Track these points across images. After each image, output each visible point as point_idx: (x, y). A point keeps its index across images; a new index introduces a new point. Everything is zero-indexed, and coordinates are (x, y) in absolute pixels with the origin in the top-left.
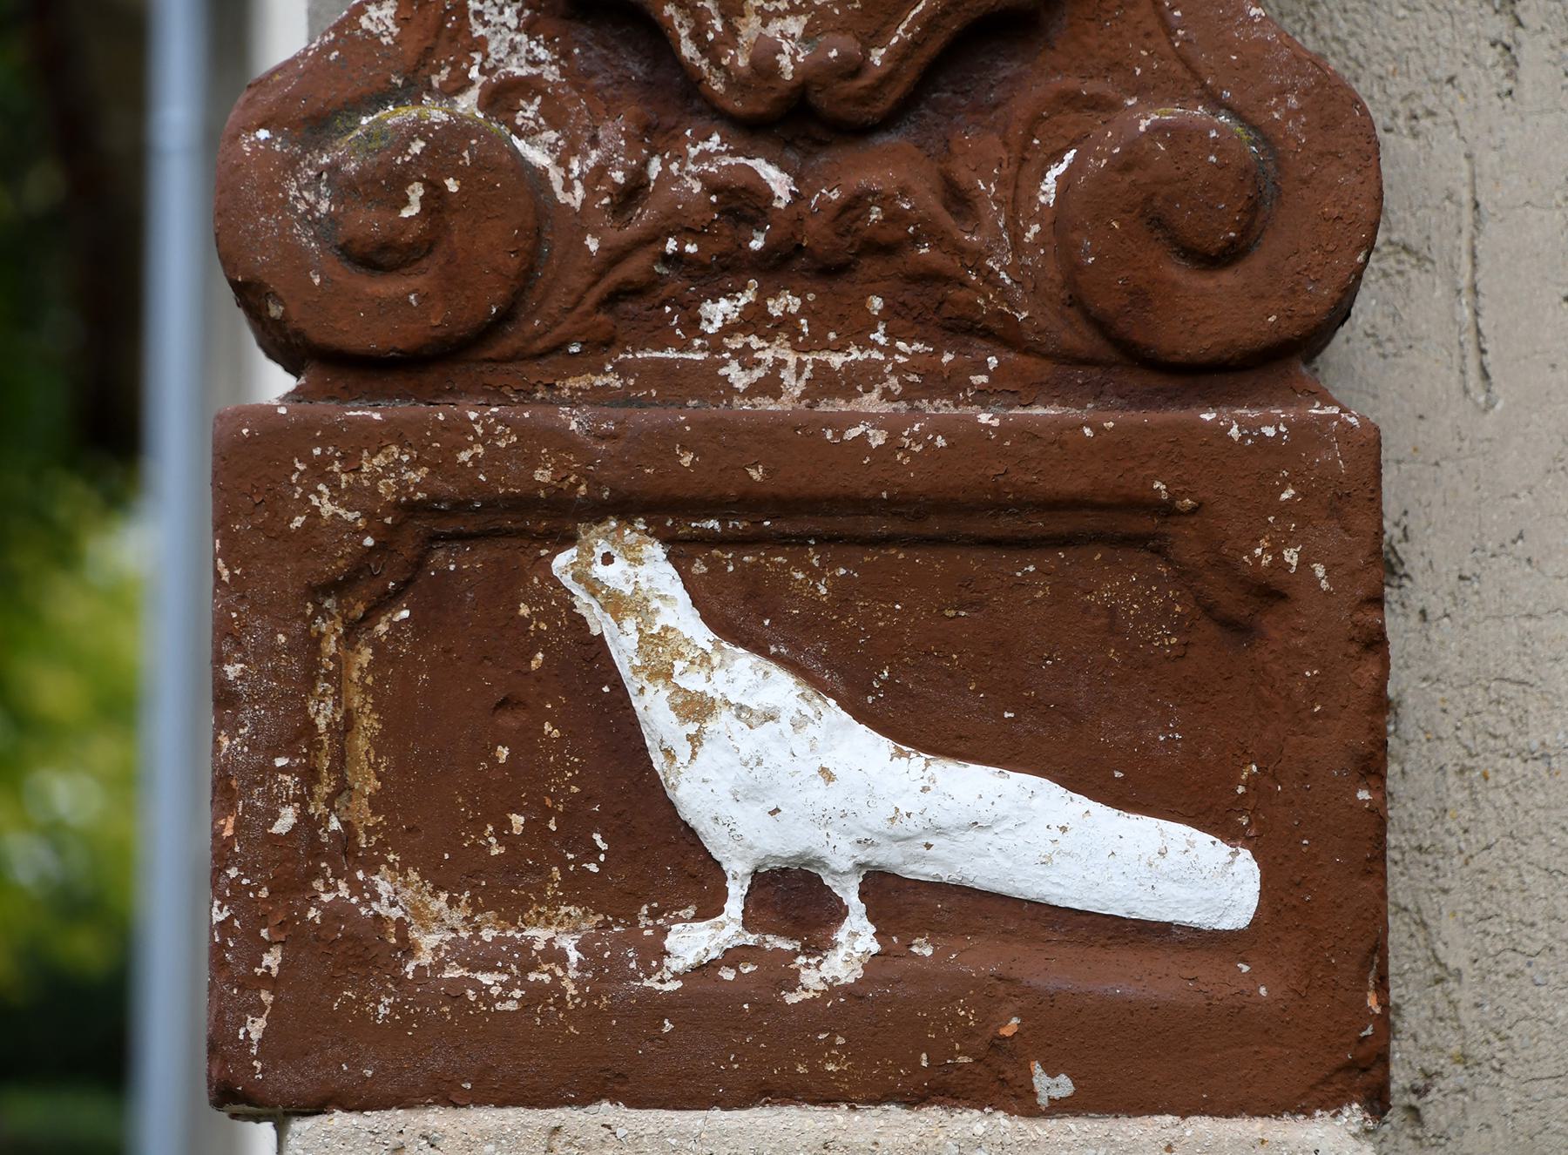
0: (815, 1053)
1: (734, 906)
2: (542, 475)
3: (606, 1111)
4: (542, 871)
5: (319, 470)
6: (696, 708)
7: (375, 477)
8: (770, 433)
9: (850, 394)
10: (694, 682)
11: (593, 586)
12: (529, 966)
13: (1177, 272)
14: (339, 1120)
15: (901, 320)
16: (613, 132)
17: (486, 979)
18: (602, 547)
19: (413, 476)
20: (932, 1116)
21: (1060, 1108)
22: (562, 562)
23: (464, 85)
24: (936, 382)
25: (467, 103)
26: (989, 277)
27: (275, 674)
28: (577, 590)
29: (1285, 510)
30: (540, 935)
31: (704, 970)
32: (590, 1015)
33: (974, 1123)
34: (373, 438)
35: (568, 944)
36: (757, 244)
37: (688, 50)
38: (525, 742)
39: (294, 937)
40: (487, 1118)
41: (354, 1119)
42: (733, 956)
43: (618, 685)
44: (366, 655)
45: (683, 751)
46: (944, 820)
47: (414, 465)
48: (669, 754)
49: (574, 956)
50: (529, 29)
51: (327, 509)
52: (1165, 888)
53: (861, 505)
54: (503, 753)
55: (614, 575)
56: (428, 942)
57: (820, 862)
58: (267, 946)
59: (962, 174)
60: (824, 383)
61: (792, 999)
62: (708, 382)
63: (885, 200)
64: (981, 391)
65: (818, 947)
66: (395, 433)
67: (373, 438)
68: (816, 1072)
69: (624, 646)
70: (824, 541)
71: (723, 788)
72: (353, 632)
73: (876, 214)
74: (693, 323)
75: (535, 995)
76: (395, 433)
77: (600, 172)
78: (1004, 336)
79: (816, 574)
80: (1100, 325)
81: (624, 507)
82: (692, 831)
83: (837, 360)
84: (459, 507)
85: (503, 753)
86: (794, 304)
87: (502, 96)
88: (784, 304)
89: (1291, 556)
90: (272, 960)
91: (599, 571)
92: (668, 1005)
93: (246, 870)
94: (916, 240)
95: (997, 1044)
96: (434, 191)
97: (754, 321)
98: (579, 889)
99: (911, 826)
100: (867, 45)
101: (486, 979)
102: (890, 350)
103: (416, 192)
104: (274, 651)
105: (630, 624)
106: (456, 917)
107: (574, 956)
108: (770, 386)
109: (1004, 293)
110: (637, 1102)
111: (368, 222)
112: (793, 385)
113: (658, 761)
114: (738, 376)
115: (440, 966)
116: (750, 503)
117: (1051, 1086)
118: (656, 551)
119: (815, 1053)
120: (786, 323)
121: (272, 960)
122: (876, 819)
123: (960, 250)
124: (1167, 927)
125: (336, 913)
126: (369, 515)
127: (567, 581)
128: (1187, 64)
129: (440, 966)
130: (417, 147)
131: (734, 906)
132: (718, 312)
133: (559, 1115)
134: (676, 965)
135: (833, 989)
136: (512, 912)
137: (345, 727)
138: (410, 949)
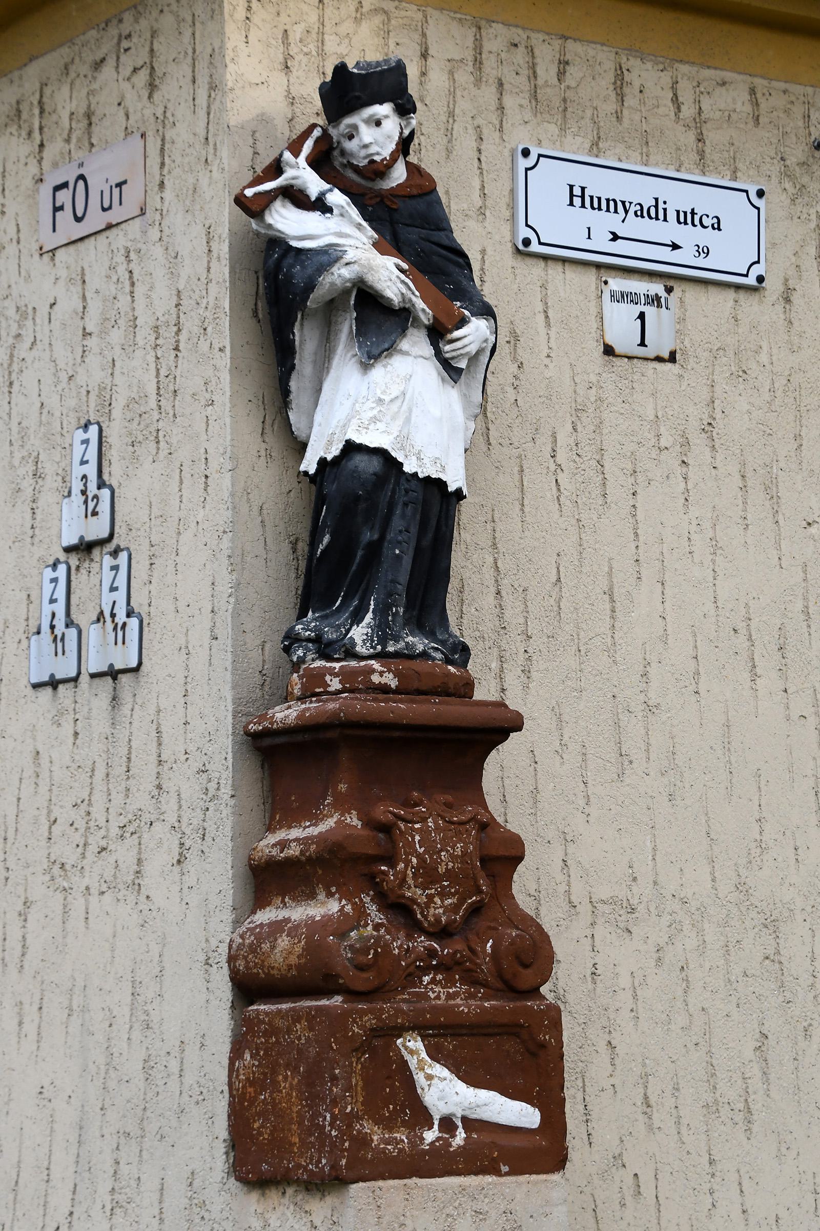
0: (457, 1163)
1: (436, 1127)
2: (399, 1021)
3: (415, 1180)
4: (396, 1119)
5: (354, 1021)
6: (429, 1077)
7: (366, 1022)
8: (435, 1009)
9: (454, 999)
10: (429, 1071)
11: (406, 1048)
12: (397, 1144)
13: (521, 969)
14: (361, 1184)
15: (463, 981)
16: (402, 934)
17: (389, 1147)
18: (408, 1038)
19: (373, 1022)
20: (481, 1177)
21: (507, 1174)
22: (399, 1041)
23: (367, 925)
24: (472, 996)
25: (370, 928)
26: (482, 970)
27: (346, 1072)
28: (402, 1049)
29: (546, 1026)
30: (397, 1135)
31: (432, 1143)
32: (411, 1156)
33: (489, 1179)
34: (363, 1013)
35: (404, 1137)
36: (434, 963)
37: (419, 916)
38: (392, 1087)
39: (352, 1139)
40: (391, 1182)
41: (364, 1184)
42: (438, 1139)
43: (411, 1072)
44: (360, 1066)
45: (426, 1088)
46: (480, 1104)
47: (374, 1019)
48: (423, 1089)
49: (406, 1141)
50: (378, 911)
51: (356, 1030)
52: (523, 1119)
53: (462, 1026)
54: (388, 1090)
55: (411, 1044)
56: (375, 1138)
57: (454, 1115)
58: (345, 1141)
59: (473, 946)
60: (450, 996)
61: (452, 1149)
62: (425, 996)
63: (461, 952)
64: (480, 998)
65: (453, 1136)
66: (370, 1011)
67: (363, 1013)
68: (457, 1167)
69: (413, 1062)
70: (451, 1035)
71: (436, 1097)
72: (359, 1059)
73: (459, 955)
74: (421, 982)
75: (400, 1150)
76: (370, 1011)
77: (401, 945)
78: (485, 985)
79: (449, 1043)
80: (505, 982)
81: (413, 1029)
82: (426, 1108)
83: (451, 991)
84: (382, 1029)
85: (388, 1090)
86: (441, 977)
87: (377, 927)
88: (439, 977)
89: (547, 1037)
90: (347, 1144)
91: (408, 1044)
92: (425, 1152)
93: (341, 1122)
94: (466, 961)
95: (493, 1159)
96: (376, 951)
97: (433, 981)
98: (405, 1124)
99: (473, 1105)
100: (457, 913)
101: (389, 1147)
102: (461, 988)
103: (372, 951)
104: (346, 1066)
105: (415, 1057)
106: (379, 1132)
107: (406, 1141)
108: (438, 997)
109: (485, 975)
110: (421, 1177)
111: (362, 959)
112: (443, 997)
113: (419, 1091)
114: (432, 995)
115: (379, 1144)
116: (441, 1026)
117: (505, 1169)
118: (419, 1038)
119: (457, 1163)
120: (440, 981)
121: (347, 1144)
122: (466, 1104)
123: (476, 964)
124: (521, 1128)
125: (359, 1132)
126: (364, 1032)
127: (400, 1046)
128: (510, 919)
129: (379, 1144)
130: (372, 941)
131: (436, 1127)
132: (426, 979)
133: (406, 1181)
134: (427, 1142)
135: (459, 1147)
136: (391, 1131)
137: (356, 1085)
138: (372, 1140)
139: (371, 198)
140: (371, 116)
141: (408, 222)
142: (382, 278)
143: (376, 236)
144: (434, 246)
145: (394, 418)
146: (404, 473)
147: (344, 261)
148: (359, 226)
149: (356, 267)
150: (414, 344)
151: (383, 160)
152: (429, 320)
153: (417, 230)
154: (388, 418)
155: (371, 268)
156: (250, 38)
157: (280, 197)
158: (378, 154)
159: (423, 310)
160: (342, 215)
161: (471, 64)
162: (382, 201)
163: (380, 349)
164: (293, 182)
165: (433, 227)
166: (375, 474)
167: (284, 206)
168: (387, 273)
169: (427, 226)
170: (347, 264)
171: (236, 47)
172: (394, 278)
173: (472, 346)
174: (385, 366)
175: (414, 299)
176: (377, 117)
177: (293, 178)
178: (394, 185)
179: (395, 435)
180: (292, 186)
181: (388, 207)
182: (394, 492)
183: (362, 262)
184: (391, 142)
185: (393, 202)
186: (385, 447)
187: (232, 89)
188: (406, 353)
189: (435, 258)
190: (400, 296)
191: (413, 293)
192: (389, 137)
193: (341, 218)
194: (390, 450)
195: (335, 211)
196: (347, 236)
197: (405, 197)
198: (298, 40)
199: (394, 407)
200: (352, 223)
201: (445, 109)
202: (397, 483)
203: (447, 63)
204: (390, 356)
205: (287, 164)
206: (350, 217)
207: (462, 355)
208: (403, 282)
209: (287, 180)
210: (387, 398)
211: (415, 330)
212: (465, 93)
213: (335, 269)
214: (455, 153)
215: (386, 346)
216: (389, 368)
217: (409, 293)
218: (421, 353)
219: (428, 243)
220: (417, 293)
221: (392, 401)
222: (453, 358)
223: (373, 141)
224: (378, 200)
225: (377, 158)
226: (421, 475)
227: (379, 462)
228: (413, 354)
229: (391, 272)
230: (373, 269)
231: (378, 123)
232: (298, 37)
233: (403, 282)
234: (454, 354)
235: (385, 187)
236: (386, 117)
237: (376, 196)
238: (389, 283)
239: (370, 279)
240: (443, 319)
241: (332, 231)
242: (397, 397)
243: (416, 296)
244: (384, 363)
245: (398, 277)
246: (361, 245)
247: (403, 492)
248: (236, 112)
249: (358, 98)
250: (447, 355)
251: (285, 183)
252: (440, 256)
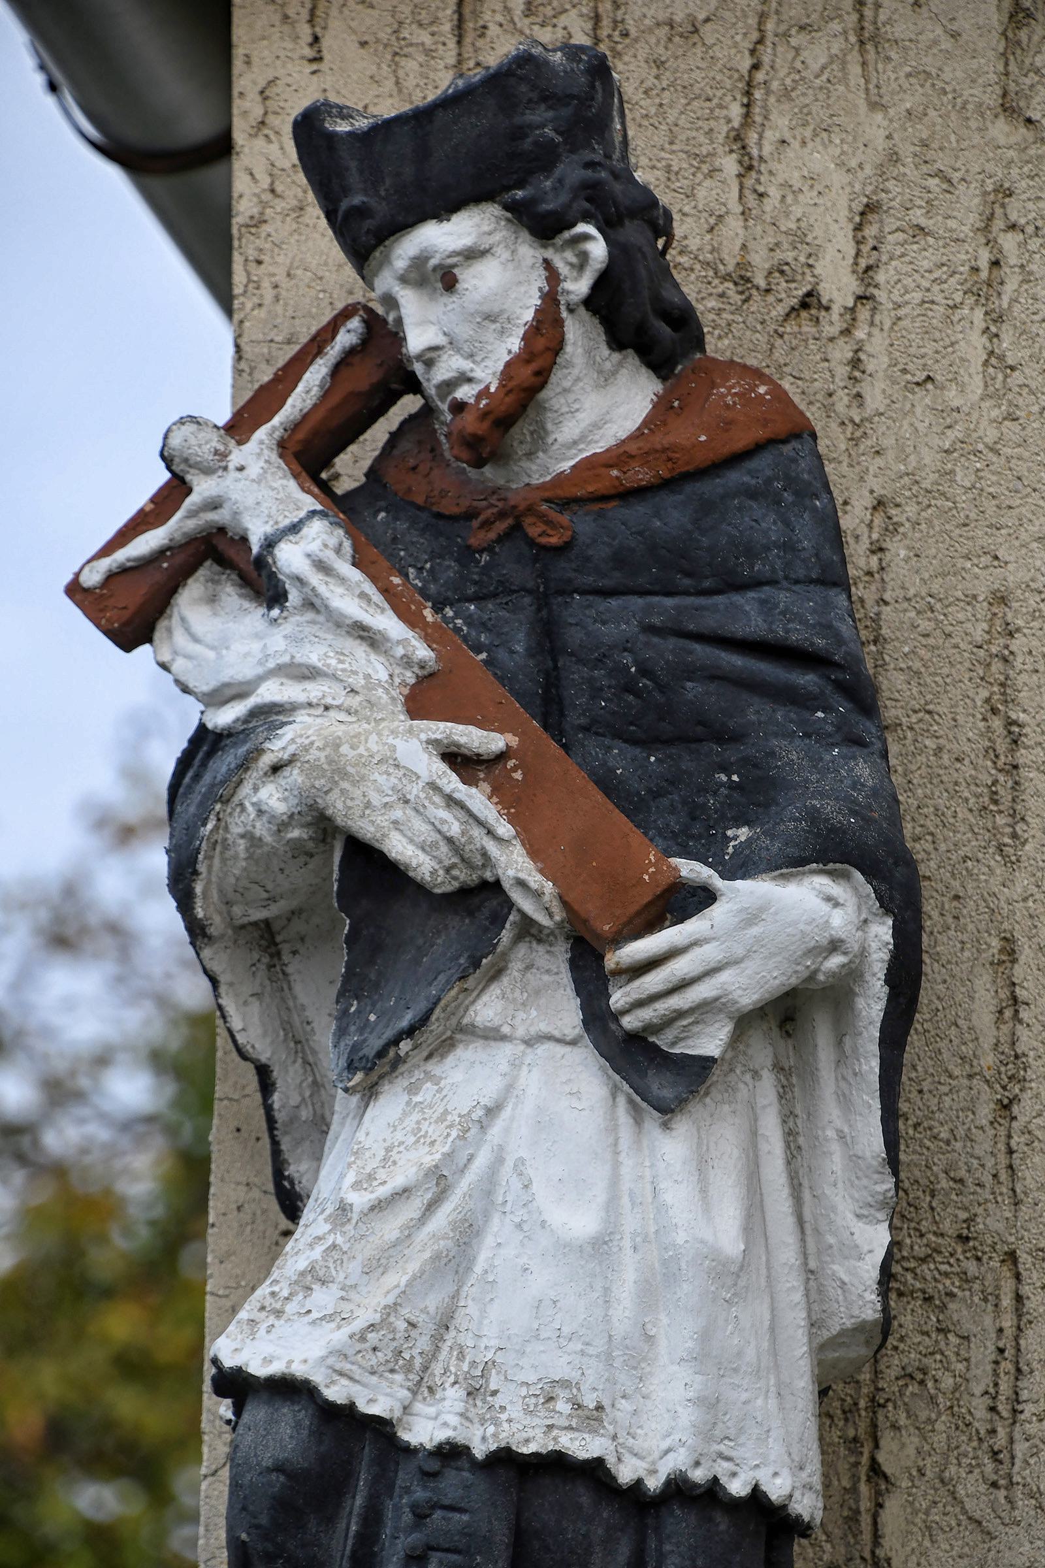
139: (487, 524)
140: (419, 261)
142: (376, 799)
143: (422, 652)
144: (698, 647)
145: (376, 1267)
146: (408, 1451)
147: (267, 760)
148: (363, 633)
149: (294, 776)
151: (479, 397)
152: (551, 915)
153: (638, 602)
154: (354, 1268)
155: (338, 772)
156: (326, 43)
157: (207, 570)
159: (521, 884)
162: (517, 527)
163: (389, 1034)
165: (707, 584)
166: (279, 1468)
167: (212, 600)
170: (276, 769)
171: (272, 82)
172: (415, 791)
173: (725, 977)
174: (413, 1089)
175: (492, 848)
176: (433, 262)
177: (214, 504)
178: (566, 465)
179: (358, 1325)
180: (222, 530)
181: (532, 543)
182: (372, 1518)
183: (313, 755)
184: (502, 332)
185: (549, 523)
186: (299, 1370)
187: (258, 222)
188: (493, 1035)
189: (693, 689)
190: (444, 848)
191: (490, 832)
192: (490, 318)
193: (310, 615)
194: (318, 1378)
196: (308, 674)
199: (390, 1228)
200: (338, 625)
202: (383, 1487)
204: (445, 1046)
207: (680, 1014)
208: (452, 802)
209: (192, 514)
210: (359, 1200)
211: (541, 949)
216: (427, 1092)
217: (477, 832)
218: (543, 1027)
219: (672, 642)
220: (505, 829)
221: (378, 1207)
222: (656, 1028)
223: (441, 340)
224: (501, 526)
225: (465, 393)
226: (479, 1451)
227: (298, 1425)
228: (521, 1032)
230: (345, 775)
231: (449, 282)
233: (452, 802)
234: (646, 1015)
235: (536, 480)
236: (472, 255)
237: (502, 515)
238: (398, 813)
239: (336, 806)
240: (589, 908)
242: (405, 1192)
244: (418, 1074)
245: (433, 786)
247: (407, 1517)
248: (268, 293)
250: (630, 1022)
251: (191, 524)
252: (716, 676)
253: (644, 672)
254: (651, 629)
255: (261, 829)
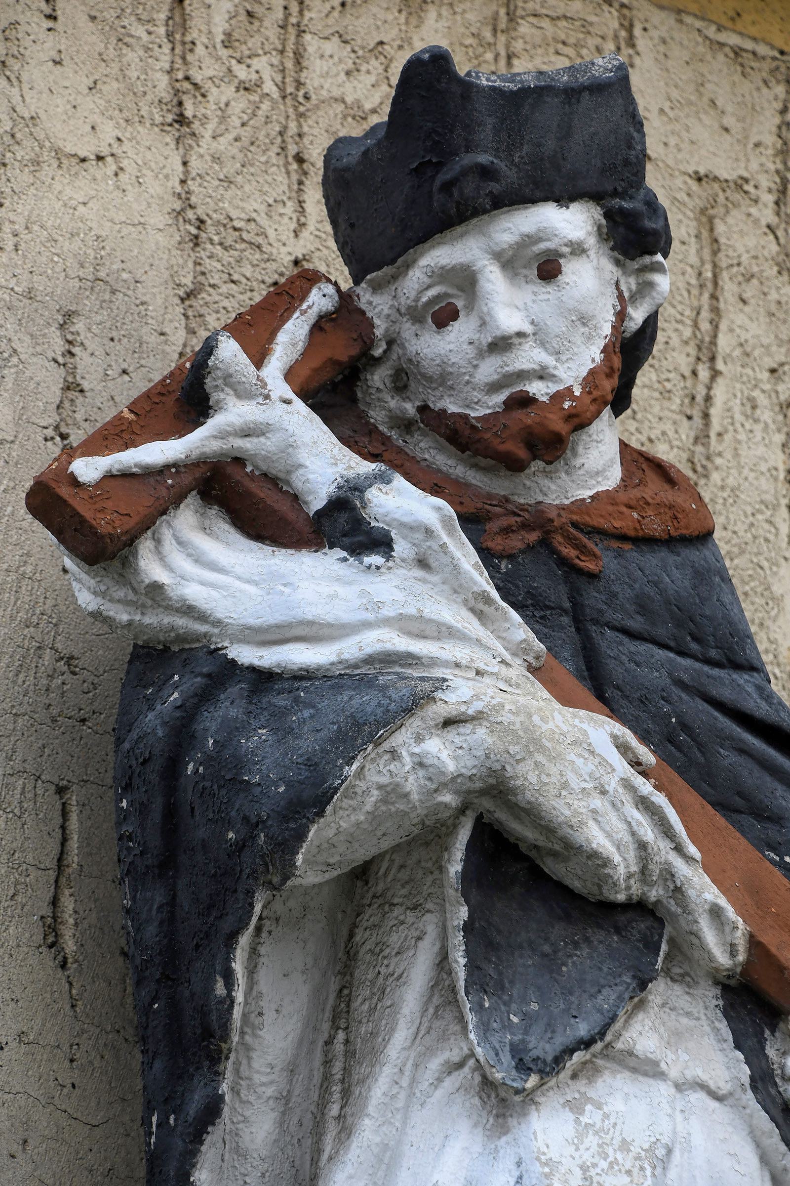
139: (507, 531)
140: (529, 240)
141: (636, 623)
142: (575, 783)
147: (438, 711)
149: (481, 734)
150: (675, 1038)
151: (557, 398)
152: (733, 953)
158: (542, 375)
159: (716, 912)
160: (422, 563)
161: (769, 199)
162: (545, 543)
163: (561, 1040)
164: (248, 445)
165: (713, 653)
168: (587, 766)
169: (694, 646)
170: (448, 723)
172: (613, 784)
175: (679, 864)
177: (247, 433)
178: (586, 493)
180: (239, 461)
181: (563, 562)
183: (506, 717)
184: (589, 338)
189: (728, 758)
190: (631, 855)
191: (679, 849)
193: (419, 573)
195: (401, 547)
197: (623, 538)
198: (220, 37)
201: (687, 332)
203: (694, 185)
205: (228, 378)
206: (456, 568)
209: (222, 435)
212: (750, 291)
213: (402, 738)
214: (716, 477)
215: (583, 1029)
216: (590, 1115)
220: (692, 850)
223: (528, 328)
224: (533, 537)
225: (539, 389)
229: (604, 762)
230: (541, 748)
232: (220, 27)
233: (644, 804)
236: (578, 250)
237: (526, 526)
238: (597, 802)
241: (388, 612)
243: (689, 859)
246: (494, 667)
249: (486, 173)
251: (216, 446)
252: (743, 751)
253: (684, 726)
254: (680, 684)
255: (413, 785)
